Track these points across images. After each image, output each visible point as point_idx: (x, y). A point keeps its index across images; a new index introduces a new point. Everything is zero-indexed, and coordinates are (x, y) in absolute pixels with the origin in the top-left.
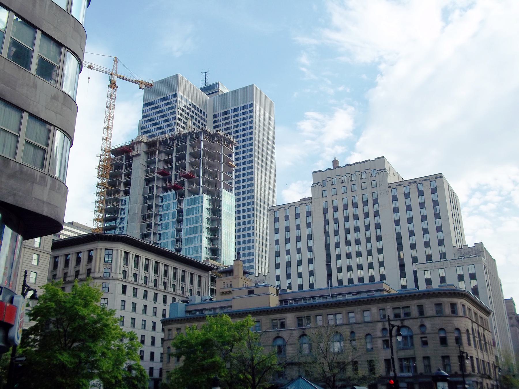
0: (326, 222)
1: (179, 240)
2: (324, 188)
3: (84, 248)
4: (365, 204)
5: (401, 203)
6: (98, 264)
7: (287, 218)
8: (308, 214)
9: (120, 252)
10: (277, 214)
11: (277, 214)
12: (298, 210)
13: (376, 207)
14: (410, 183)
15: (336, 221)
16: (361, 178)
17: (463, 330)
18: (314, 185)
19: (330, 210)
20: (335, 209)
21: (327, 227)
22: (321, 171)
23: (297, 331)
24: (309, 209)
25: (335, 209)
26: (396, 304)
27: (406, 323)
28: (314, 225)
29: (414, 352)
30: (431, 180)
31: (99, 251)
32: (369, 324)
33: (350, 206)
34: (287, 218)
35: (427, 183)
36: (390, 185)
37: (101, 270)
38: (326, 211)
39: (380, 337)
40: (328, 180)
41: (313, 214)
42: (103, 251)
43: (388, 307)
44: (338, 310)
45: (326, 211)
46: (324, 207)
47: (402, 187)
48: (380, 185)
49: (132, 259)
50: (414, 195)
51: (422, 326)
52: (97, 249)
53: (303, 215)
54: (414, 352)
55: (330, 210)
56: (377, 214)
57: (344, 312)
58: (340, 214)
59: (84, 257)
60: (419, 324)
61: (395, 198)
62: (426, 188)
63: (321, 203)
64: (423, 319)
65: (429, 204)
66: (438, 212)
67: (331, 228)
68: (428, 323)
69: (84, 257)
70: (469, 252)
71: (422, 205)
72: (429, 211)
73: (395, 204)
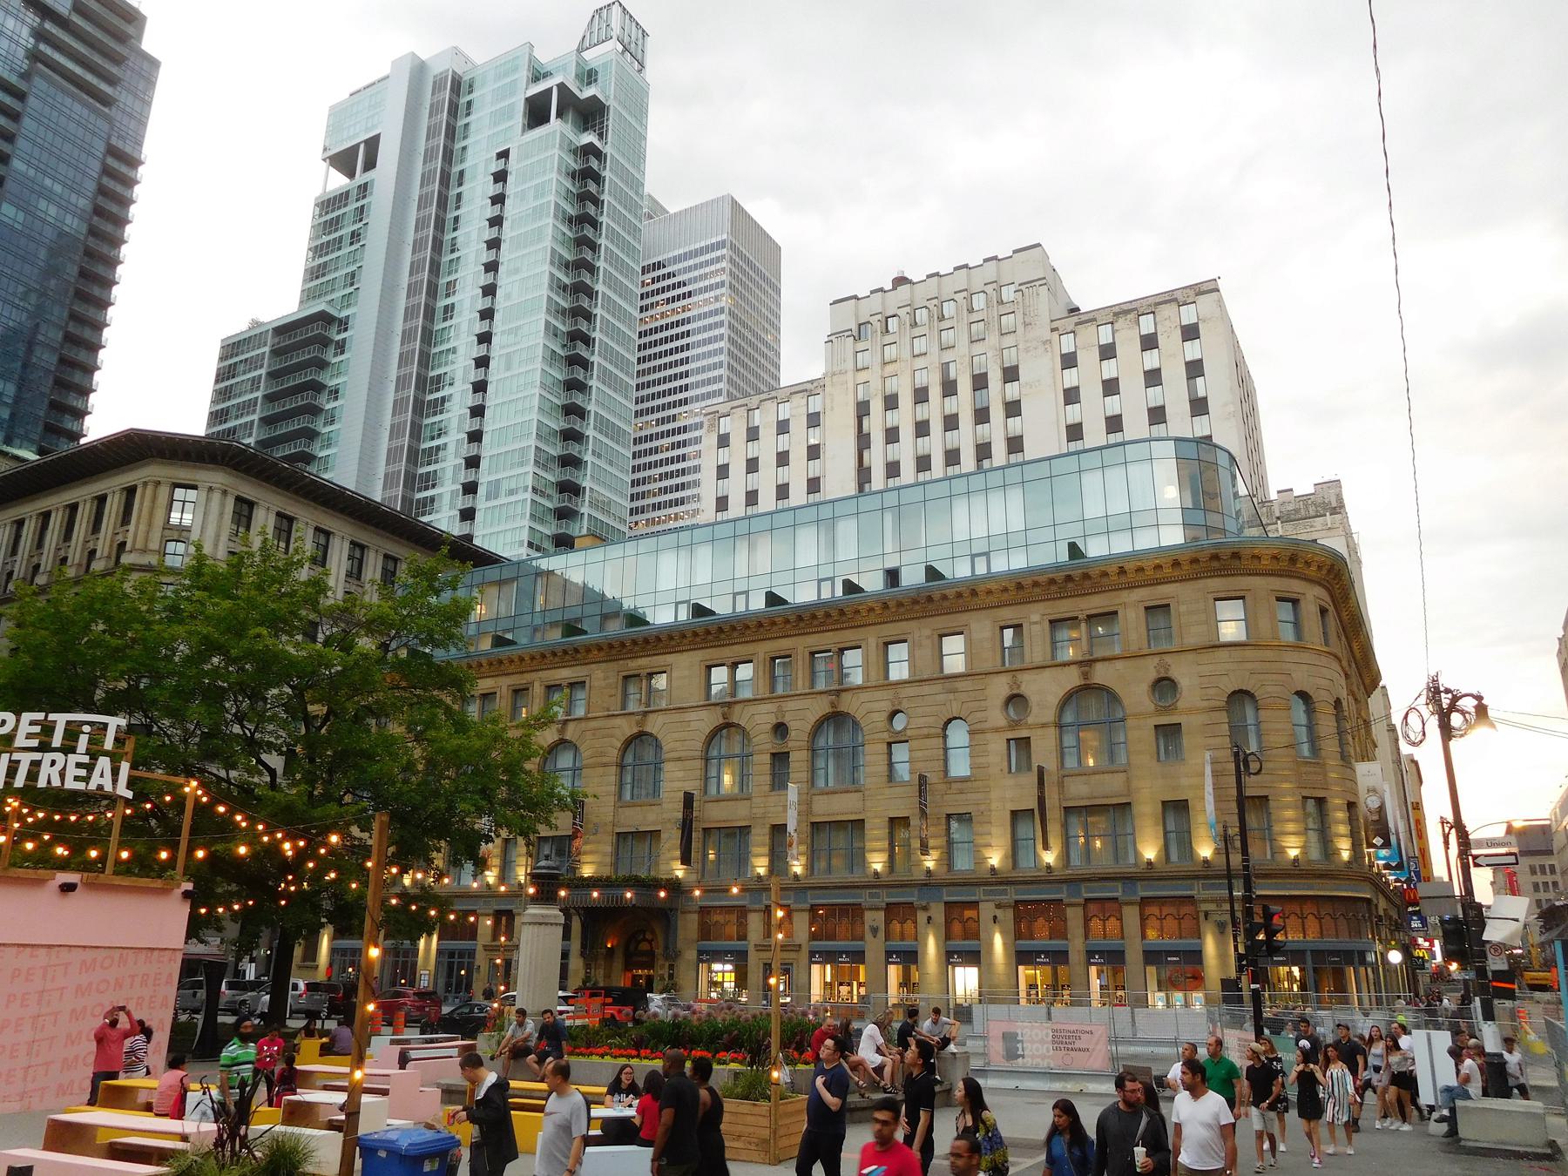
0: (863, 441)
1: (468, 515)
2: (861, 346)
3: (112, 485)
4: (980, 382)
5: (1088, 375)
6: (142, 527)
7: (753, 434)
8: (814, 420)
9: (216, 496)
10: (725, 425)
11: (725, 425)
12: (785, 412)
13: (1012, 391)
14: (1116, 314)
15: (892, 435)
16: (971, 310)
17: (1323, 701)
18: (835, 336)
19: (877, 406)
20: (891, 402)
21: (866, 454)
22: (855, 297)
23: (704, 714)
24: (816, 404)
25: (891, 402)
26: (1064, 608)
27: (1101, 674)
28: (828, 453)
29: (1128, 780)
30: (1181, 299)
31: (149, 491)
32: (961, 685)
33: (935, 392)
34: (753, 434)
35: (1167, 311)
36: (1055, 325)
37: (154, 545)
38: (863, 410)
39: (997, 730)
40: (873, 320)
41: (826, 420)
42: (164, 492)
43: (1035, 618)
44: (848, 636)
45: (863, 410)
46: (860, 398)
47: (1091, 328)
48: (1026, 325)
49: (264, 519)
50: (1128, 346)
51: (1164, 686)
52: (145, 484)
53: (798, 425)
54: (1128, 780)
55: (877, 406)
56: (1013, 409)
57: (872, 642)
58: (904, 418)
59: (113, 506)
60: (1153, 675)
61: (1069, 361)
62: (1167, 326)
63: (851, 385)
64: (1168, 658)
65: (1175, 376)
66: (1201, 394)
67: (876, 458)
68: (1185, 673)
69: (113, 506)
70: (1297, 511)
71: (1153, 377)
72: (1174, 394)
73: (1071, 378)
